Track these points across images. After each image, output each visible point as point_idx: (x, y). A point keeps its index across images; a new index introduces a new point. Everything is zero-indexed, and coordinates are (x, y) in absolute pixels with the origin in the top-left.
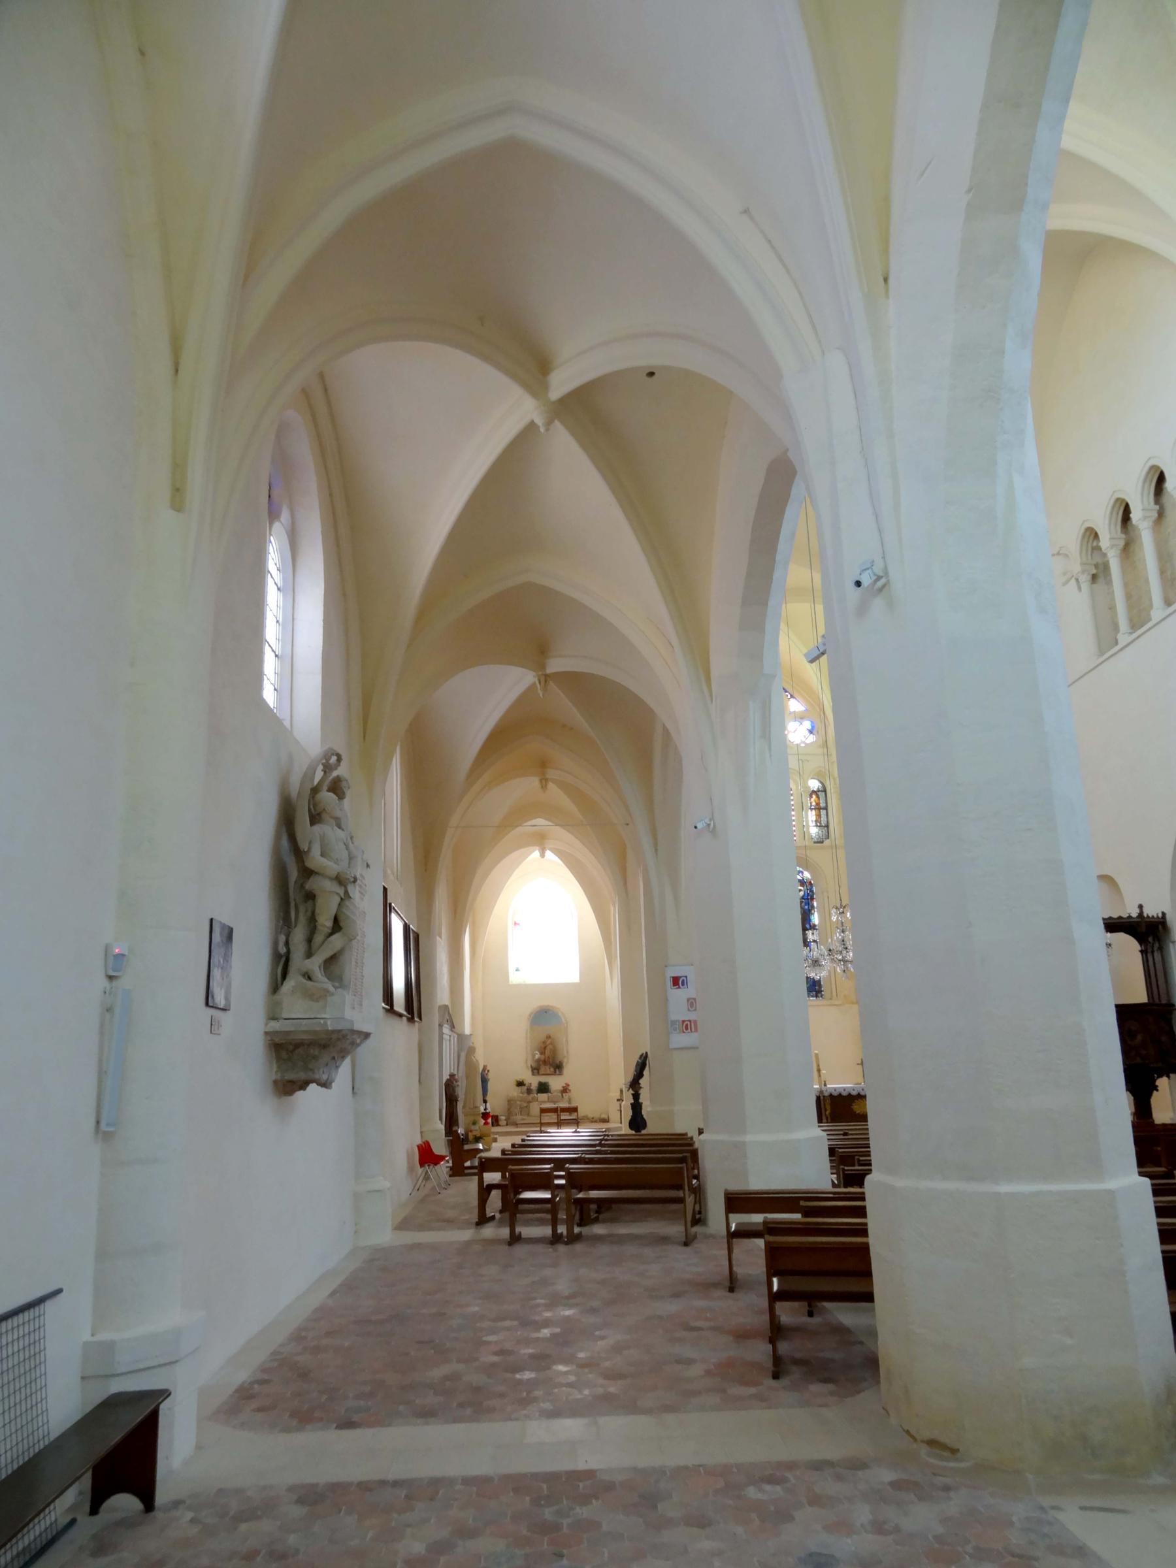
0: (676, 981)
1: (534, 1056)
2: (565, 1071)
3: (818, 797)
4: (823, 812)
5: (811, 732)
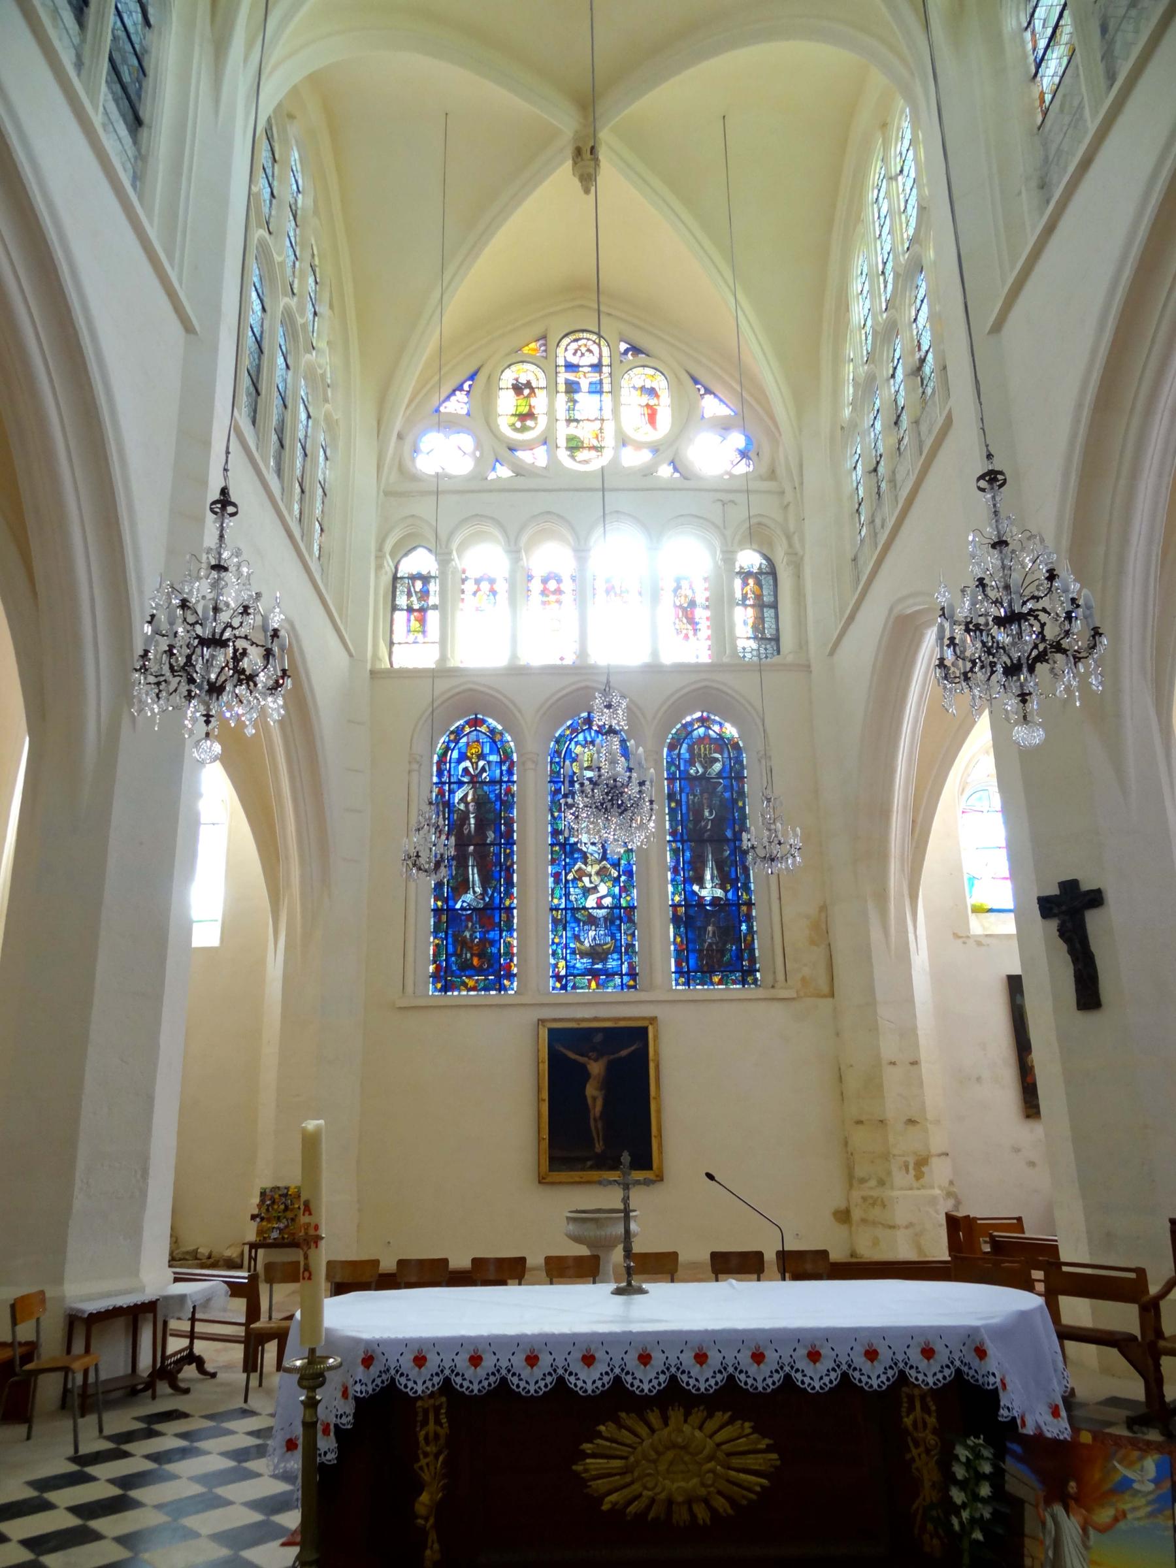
3: (759, 583)
5: (744, 454)
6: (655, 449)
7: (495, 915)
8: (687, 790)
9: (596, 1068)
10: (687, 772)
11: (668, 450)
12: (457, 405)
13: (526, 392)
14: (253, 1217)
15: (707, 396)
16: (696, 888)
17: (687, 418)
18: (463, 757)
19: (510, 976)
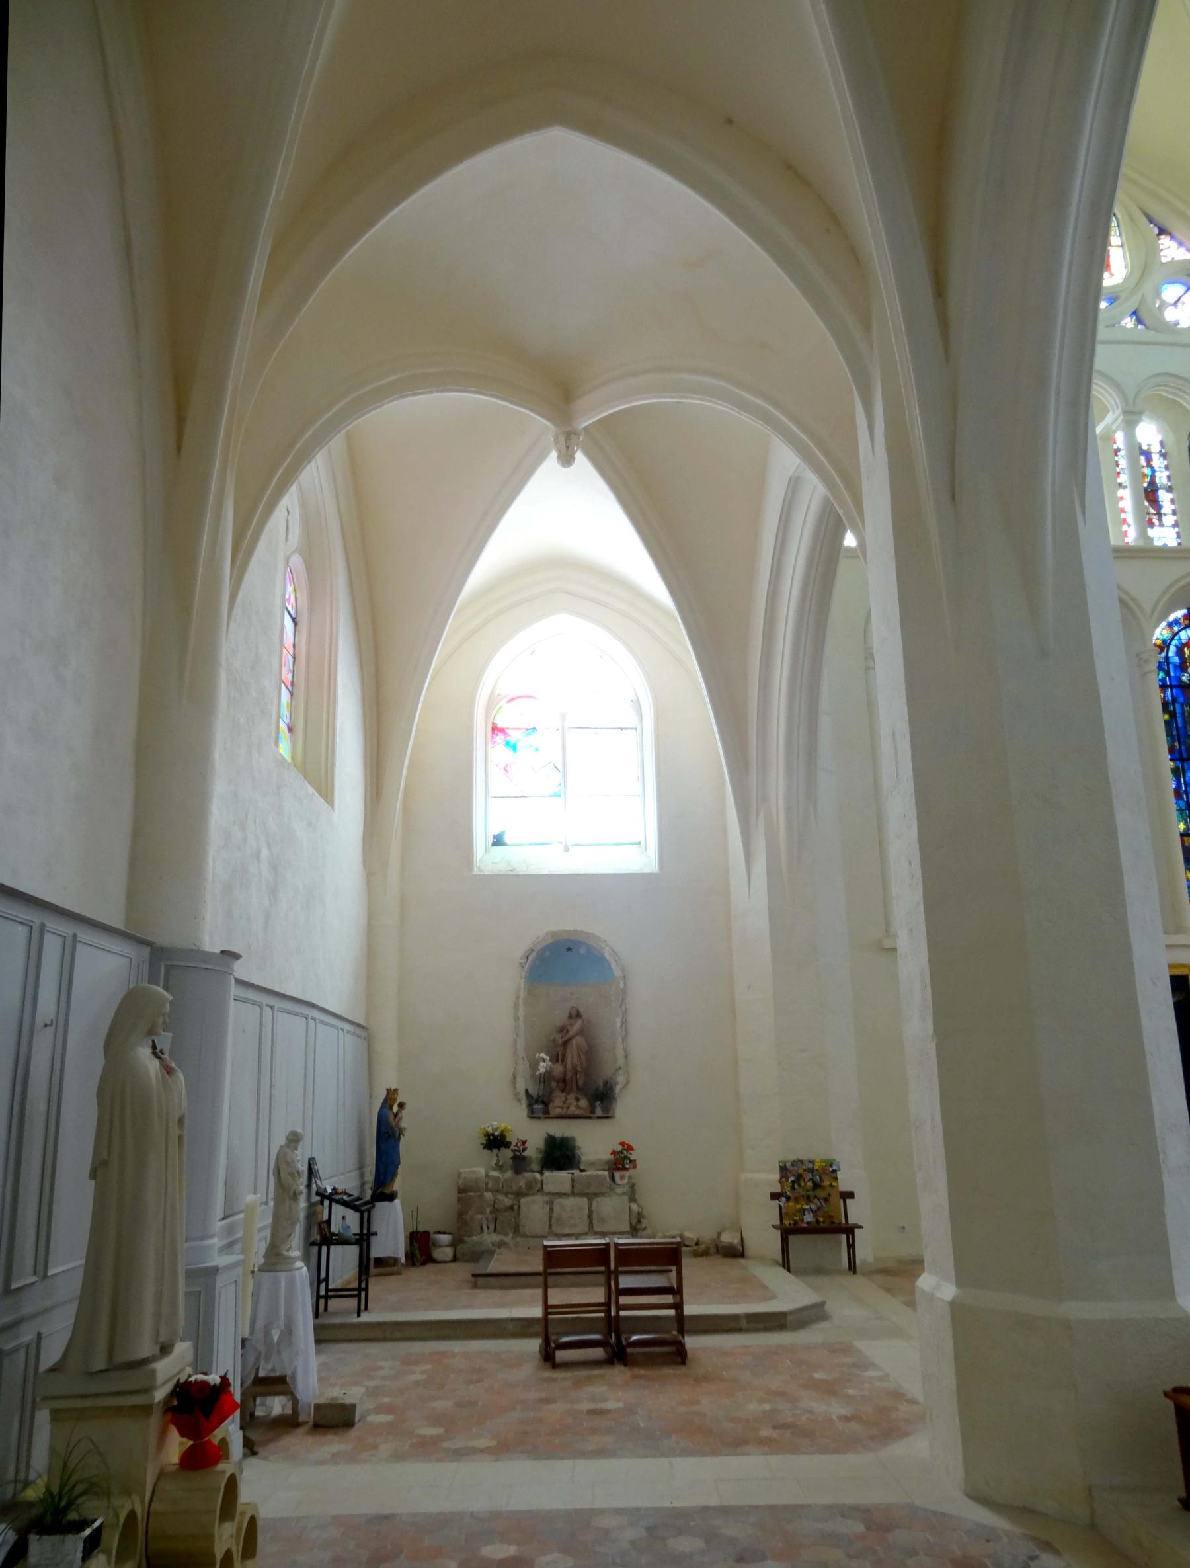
1: (534, 1065)
2: (624, 1106)
8: (1181, 700)
10: (1179, 679)
14: (774, 1196)
15: (1165, 241)
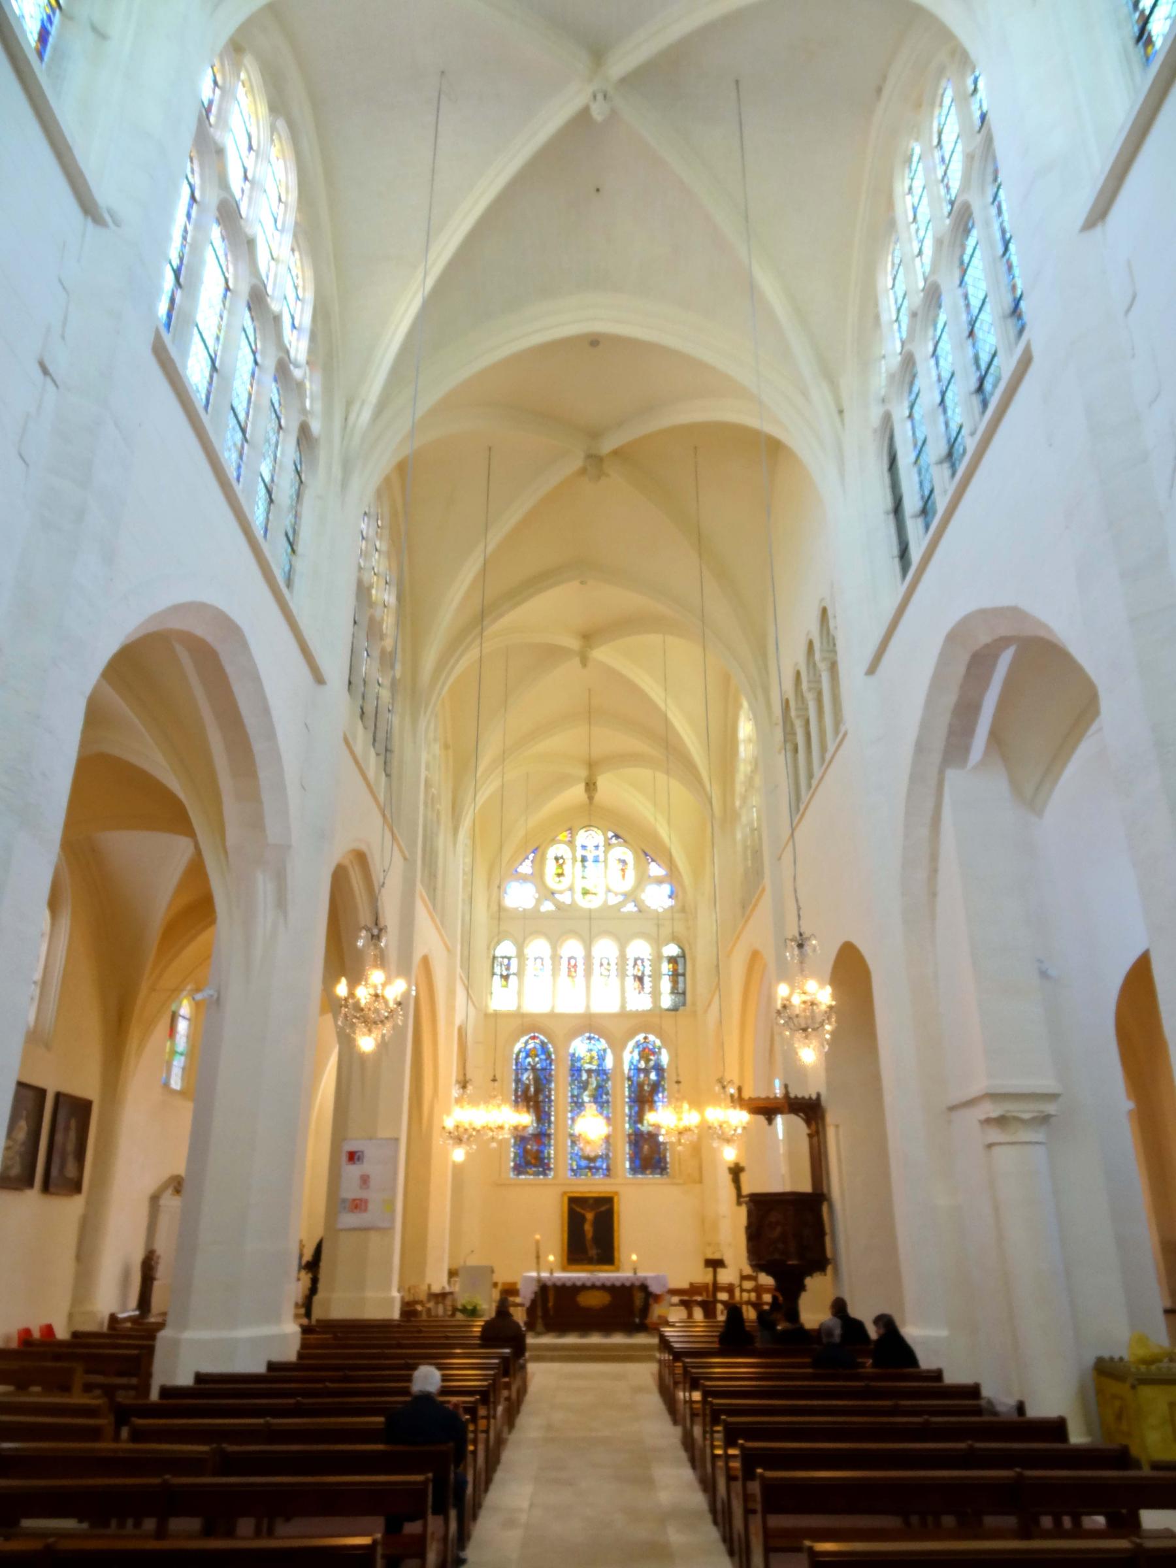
0: (353, 1157)
4: (681, 979)
6: (625, 895)
7: (541, 1137)
9: (590, 1216)
11: (630, 896)
12: (526, 868)
13: (561, 861)
16: (639, 1126)
17: (643, 879)
18: (528, 1056)
19: (550, 1169)
